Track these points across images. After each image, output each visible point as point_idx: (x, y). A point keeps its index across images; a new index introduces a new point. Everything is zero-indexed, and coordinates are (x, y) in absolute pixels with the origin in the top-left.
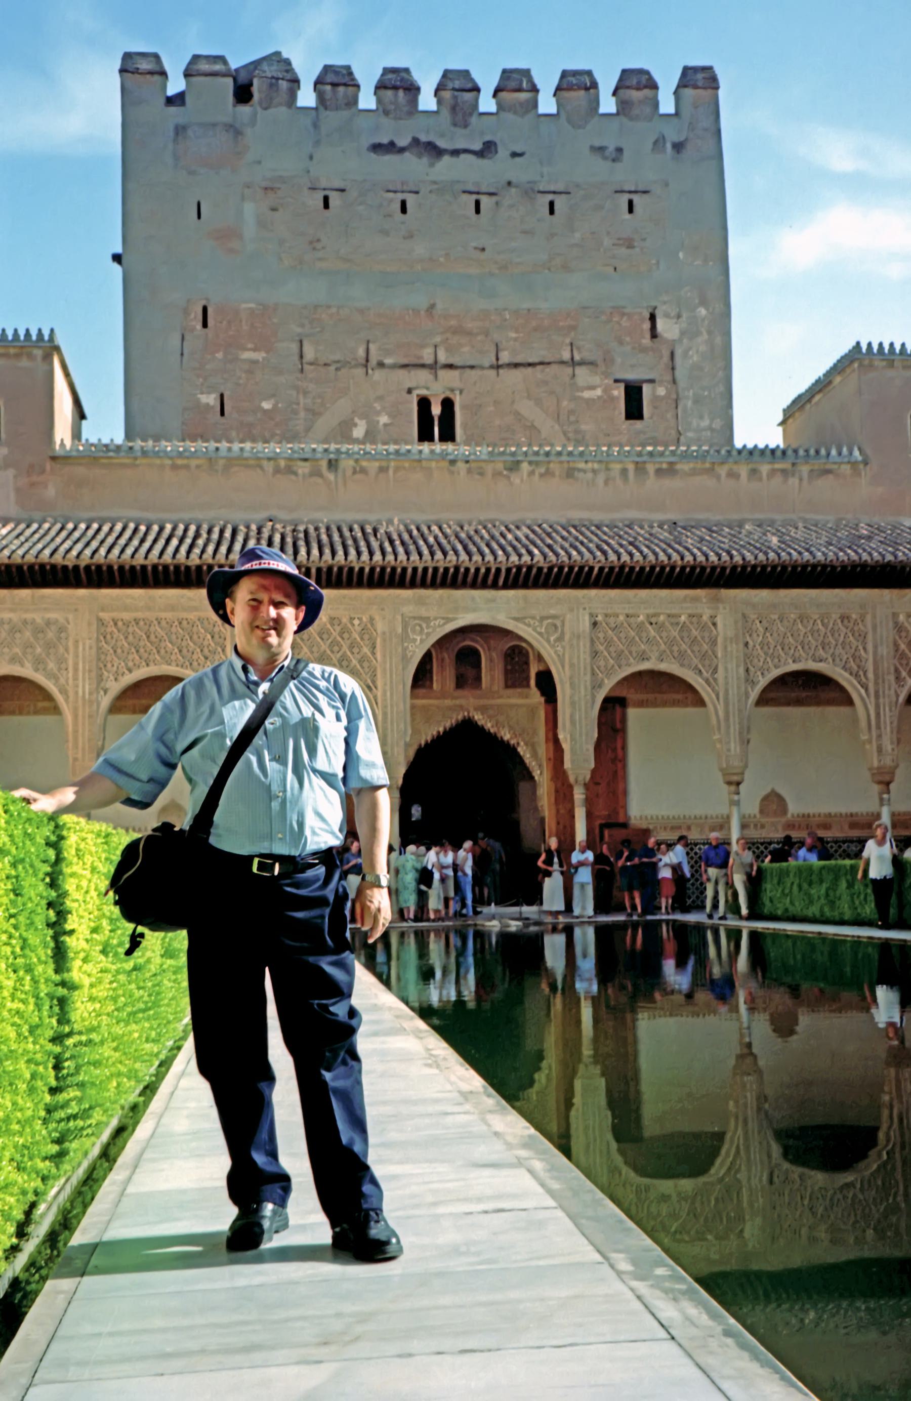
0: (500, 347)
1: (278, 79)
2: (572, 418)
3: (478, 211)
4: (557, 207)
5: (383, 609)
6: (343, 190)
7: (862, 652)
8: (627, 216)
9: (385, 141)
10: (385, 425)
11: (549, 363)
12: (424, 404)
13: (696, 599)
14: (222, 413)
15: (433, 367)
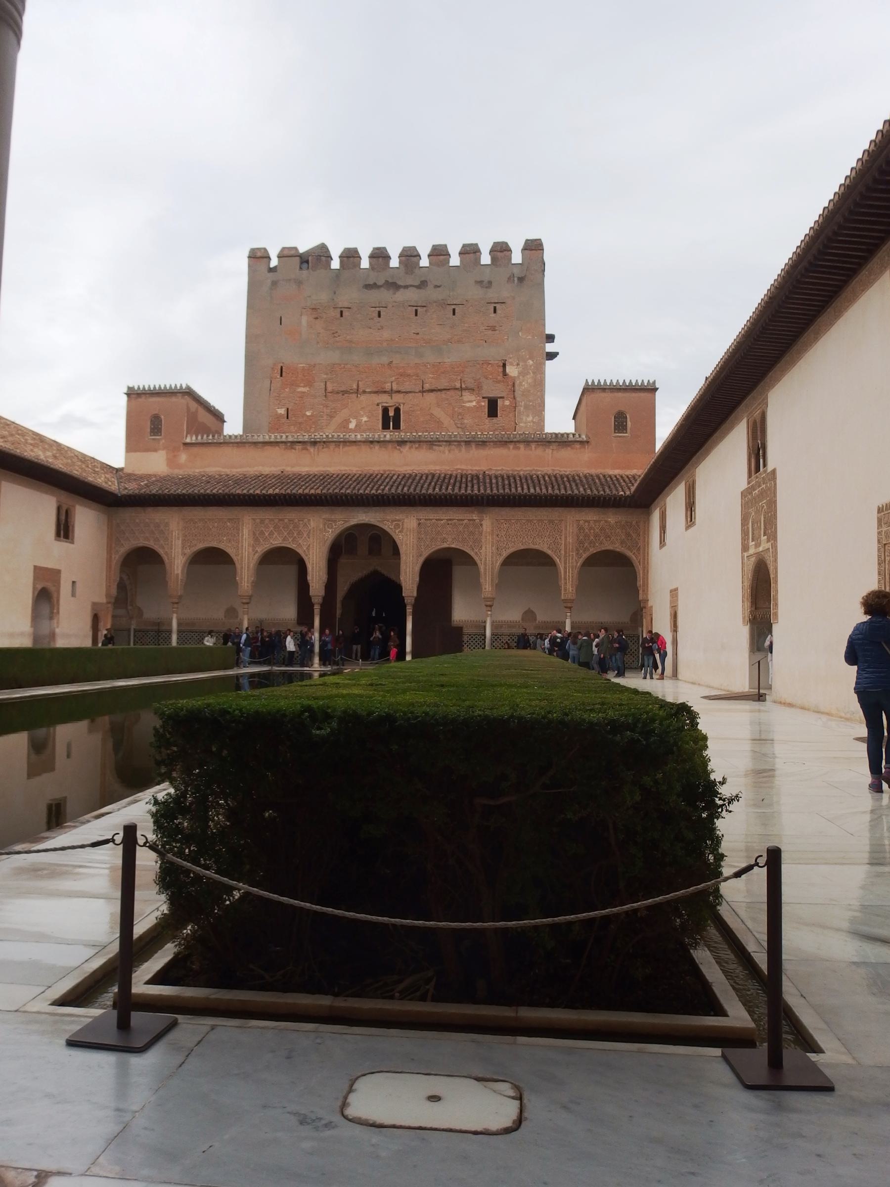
0: (425, 382)
1: (320, 256)
2: (460, 417)
3: (416, 315)
4: (456, 312)
5: (314, 516)
6: (350, 308)
7: (559, 540)
8: (493, 315)
9: (371, 283)
10: (365, 421)
11: (449, 389)
12: (385, 410)
13: (473, 512)
14: (288, 418)
15: (391, 392)
